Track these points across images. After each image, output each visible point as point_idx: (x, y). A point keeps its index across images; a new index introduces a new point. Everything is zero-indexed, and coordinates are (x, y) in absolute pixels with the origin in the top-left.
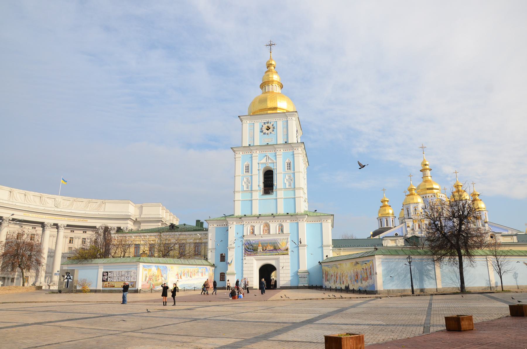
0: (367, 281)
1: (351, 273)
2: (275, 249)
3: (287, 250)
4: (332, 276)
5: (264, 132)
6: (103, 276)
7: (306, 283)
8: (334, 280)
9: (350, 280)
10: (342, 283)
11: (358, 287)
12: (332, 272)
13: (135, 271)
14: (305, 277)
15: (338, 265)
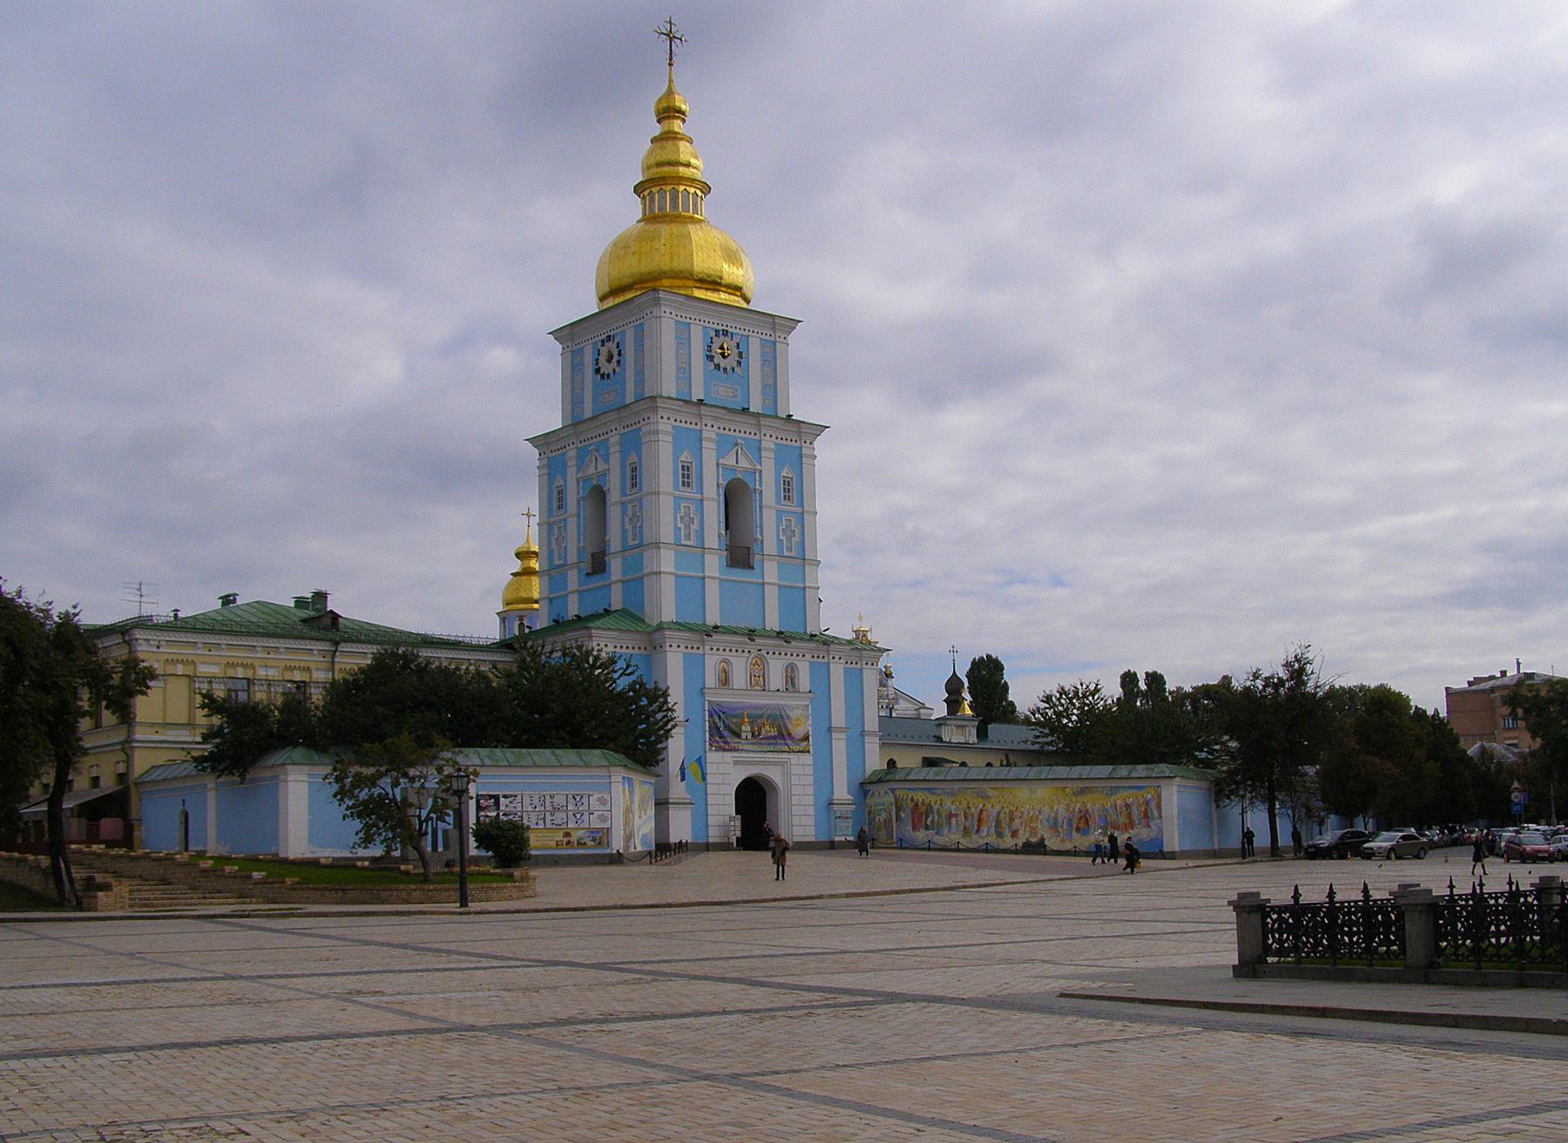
0: (1130, 831)
1: (1056, 813)
2: (781, 736)
3: (806, 738)
4: (951, 816)
5: (716, 362)
6: (479, 808)
7: (850, 833)
8: (962, 828)
9: (1051, 828)
10: (1007, 833)
11: (1086, 844)
12: (953, 807)
13: (607, 796)
14: (847, 818)
15: (988, 790)
